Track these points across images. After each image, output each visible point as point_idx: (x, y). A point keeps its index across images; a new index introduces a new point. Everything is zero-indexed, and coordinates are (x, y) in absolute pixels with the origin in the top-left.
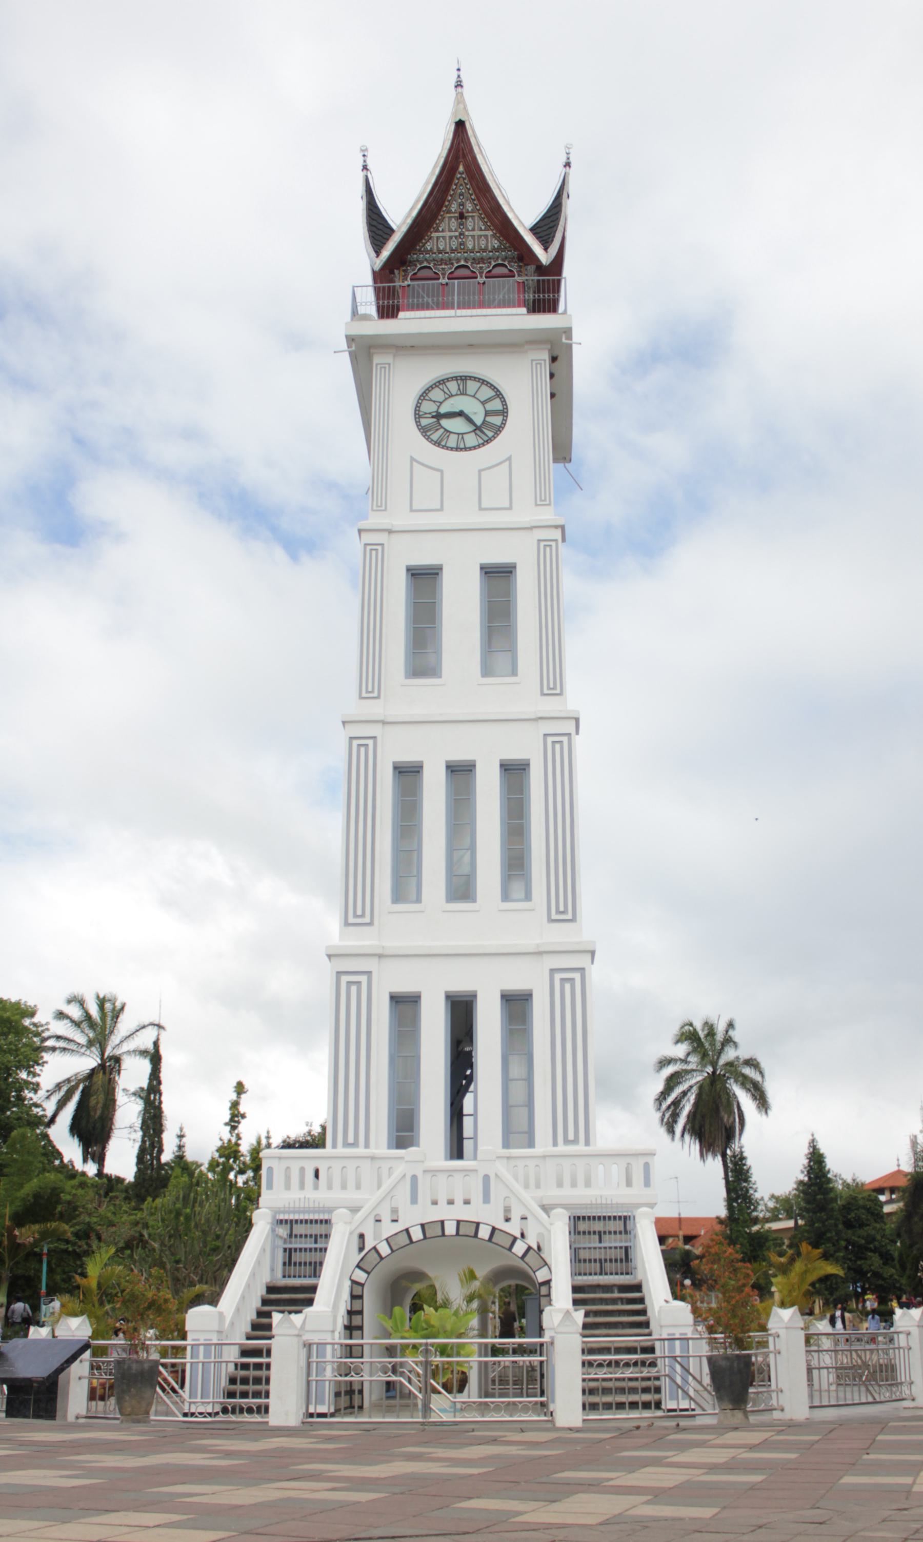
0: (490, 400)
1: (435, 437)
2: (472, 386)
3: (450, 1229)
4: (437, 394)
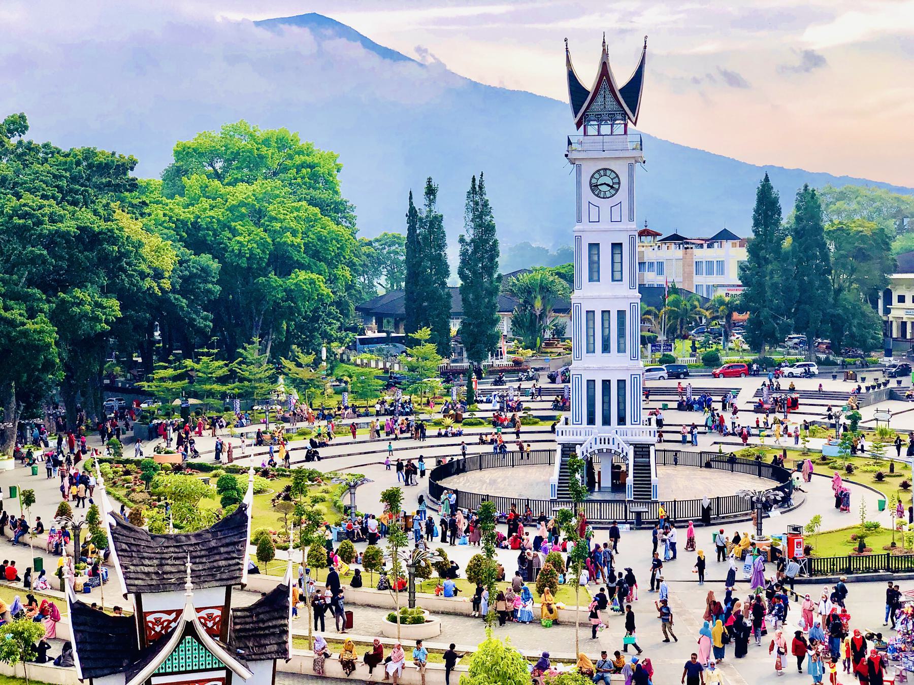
0: (615, 178)
1: (596, 193)
2: (608, 172)
3: (605, 451)
4: (597, 176)
